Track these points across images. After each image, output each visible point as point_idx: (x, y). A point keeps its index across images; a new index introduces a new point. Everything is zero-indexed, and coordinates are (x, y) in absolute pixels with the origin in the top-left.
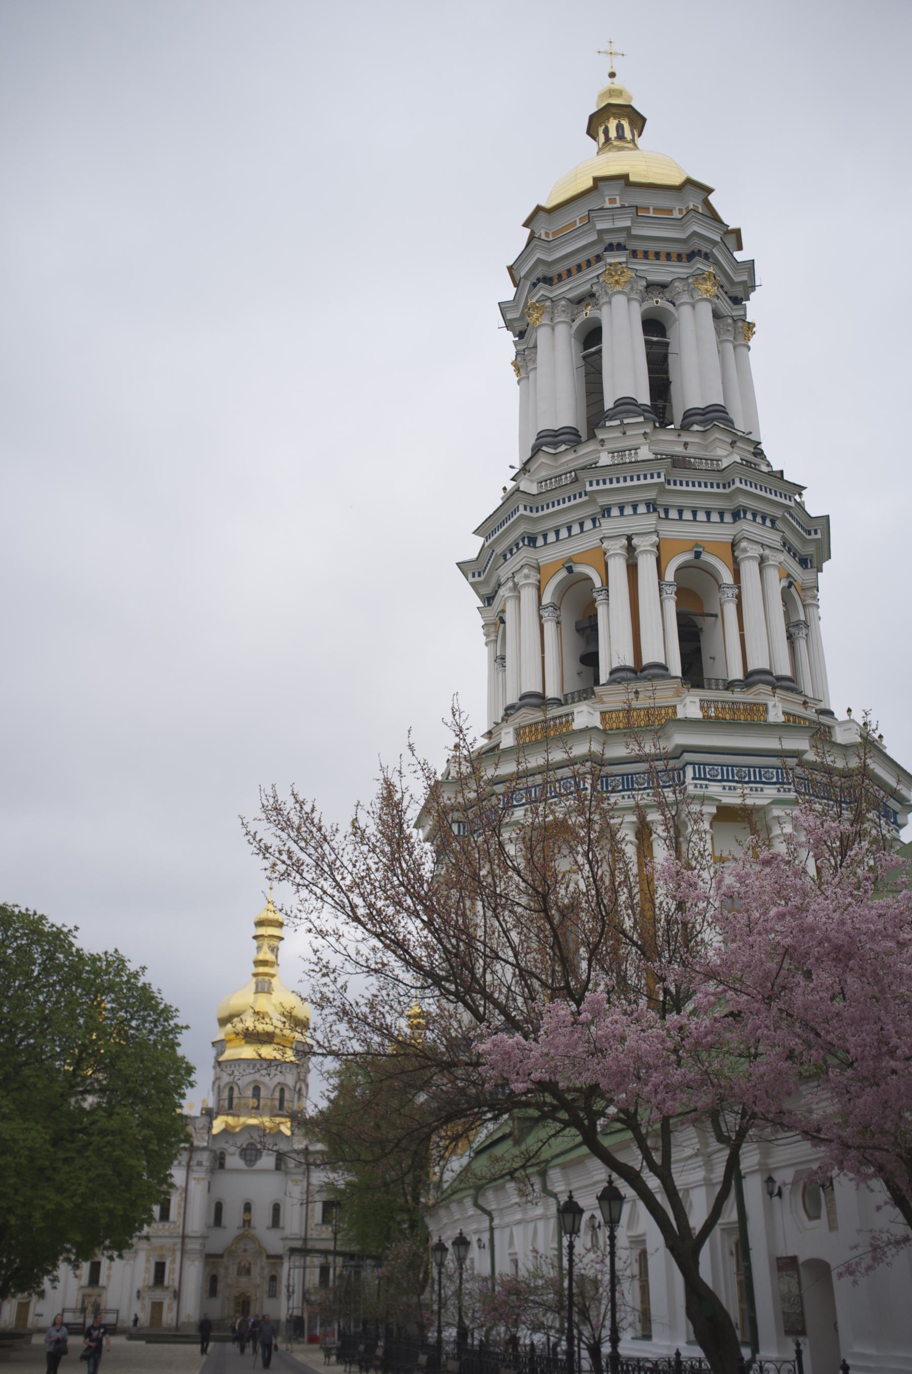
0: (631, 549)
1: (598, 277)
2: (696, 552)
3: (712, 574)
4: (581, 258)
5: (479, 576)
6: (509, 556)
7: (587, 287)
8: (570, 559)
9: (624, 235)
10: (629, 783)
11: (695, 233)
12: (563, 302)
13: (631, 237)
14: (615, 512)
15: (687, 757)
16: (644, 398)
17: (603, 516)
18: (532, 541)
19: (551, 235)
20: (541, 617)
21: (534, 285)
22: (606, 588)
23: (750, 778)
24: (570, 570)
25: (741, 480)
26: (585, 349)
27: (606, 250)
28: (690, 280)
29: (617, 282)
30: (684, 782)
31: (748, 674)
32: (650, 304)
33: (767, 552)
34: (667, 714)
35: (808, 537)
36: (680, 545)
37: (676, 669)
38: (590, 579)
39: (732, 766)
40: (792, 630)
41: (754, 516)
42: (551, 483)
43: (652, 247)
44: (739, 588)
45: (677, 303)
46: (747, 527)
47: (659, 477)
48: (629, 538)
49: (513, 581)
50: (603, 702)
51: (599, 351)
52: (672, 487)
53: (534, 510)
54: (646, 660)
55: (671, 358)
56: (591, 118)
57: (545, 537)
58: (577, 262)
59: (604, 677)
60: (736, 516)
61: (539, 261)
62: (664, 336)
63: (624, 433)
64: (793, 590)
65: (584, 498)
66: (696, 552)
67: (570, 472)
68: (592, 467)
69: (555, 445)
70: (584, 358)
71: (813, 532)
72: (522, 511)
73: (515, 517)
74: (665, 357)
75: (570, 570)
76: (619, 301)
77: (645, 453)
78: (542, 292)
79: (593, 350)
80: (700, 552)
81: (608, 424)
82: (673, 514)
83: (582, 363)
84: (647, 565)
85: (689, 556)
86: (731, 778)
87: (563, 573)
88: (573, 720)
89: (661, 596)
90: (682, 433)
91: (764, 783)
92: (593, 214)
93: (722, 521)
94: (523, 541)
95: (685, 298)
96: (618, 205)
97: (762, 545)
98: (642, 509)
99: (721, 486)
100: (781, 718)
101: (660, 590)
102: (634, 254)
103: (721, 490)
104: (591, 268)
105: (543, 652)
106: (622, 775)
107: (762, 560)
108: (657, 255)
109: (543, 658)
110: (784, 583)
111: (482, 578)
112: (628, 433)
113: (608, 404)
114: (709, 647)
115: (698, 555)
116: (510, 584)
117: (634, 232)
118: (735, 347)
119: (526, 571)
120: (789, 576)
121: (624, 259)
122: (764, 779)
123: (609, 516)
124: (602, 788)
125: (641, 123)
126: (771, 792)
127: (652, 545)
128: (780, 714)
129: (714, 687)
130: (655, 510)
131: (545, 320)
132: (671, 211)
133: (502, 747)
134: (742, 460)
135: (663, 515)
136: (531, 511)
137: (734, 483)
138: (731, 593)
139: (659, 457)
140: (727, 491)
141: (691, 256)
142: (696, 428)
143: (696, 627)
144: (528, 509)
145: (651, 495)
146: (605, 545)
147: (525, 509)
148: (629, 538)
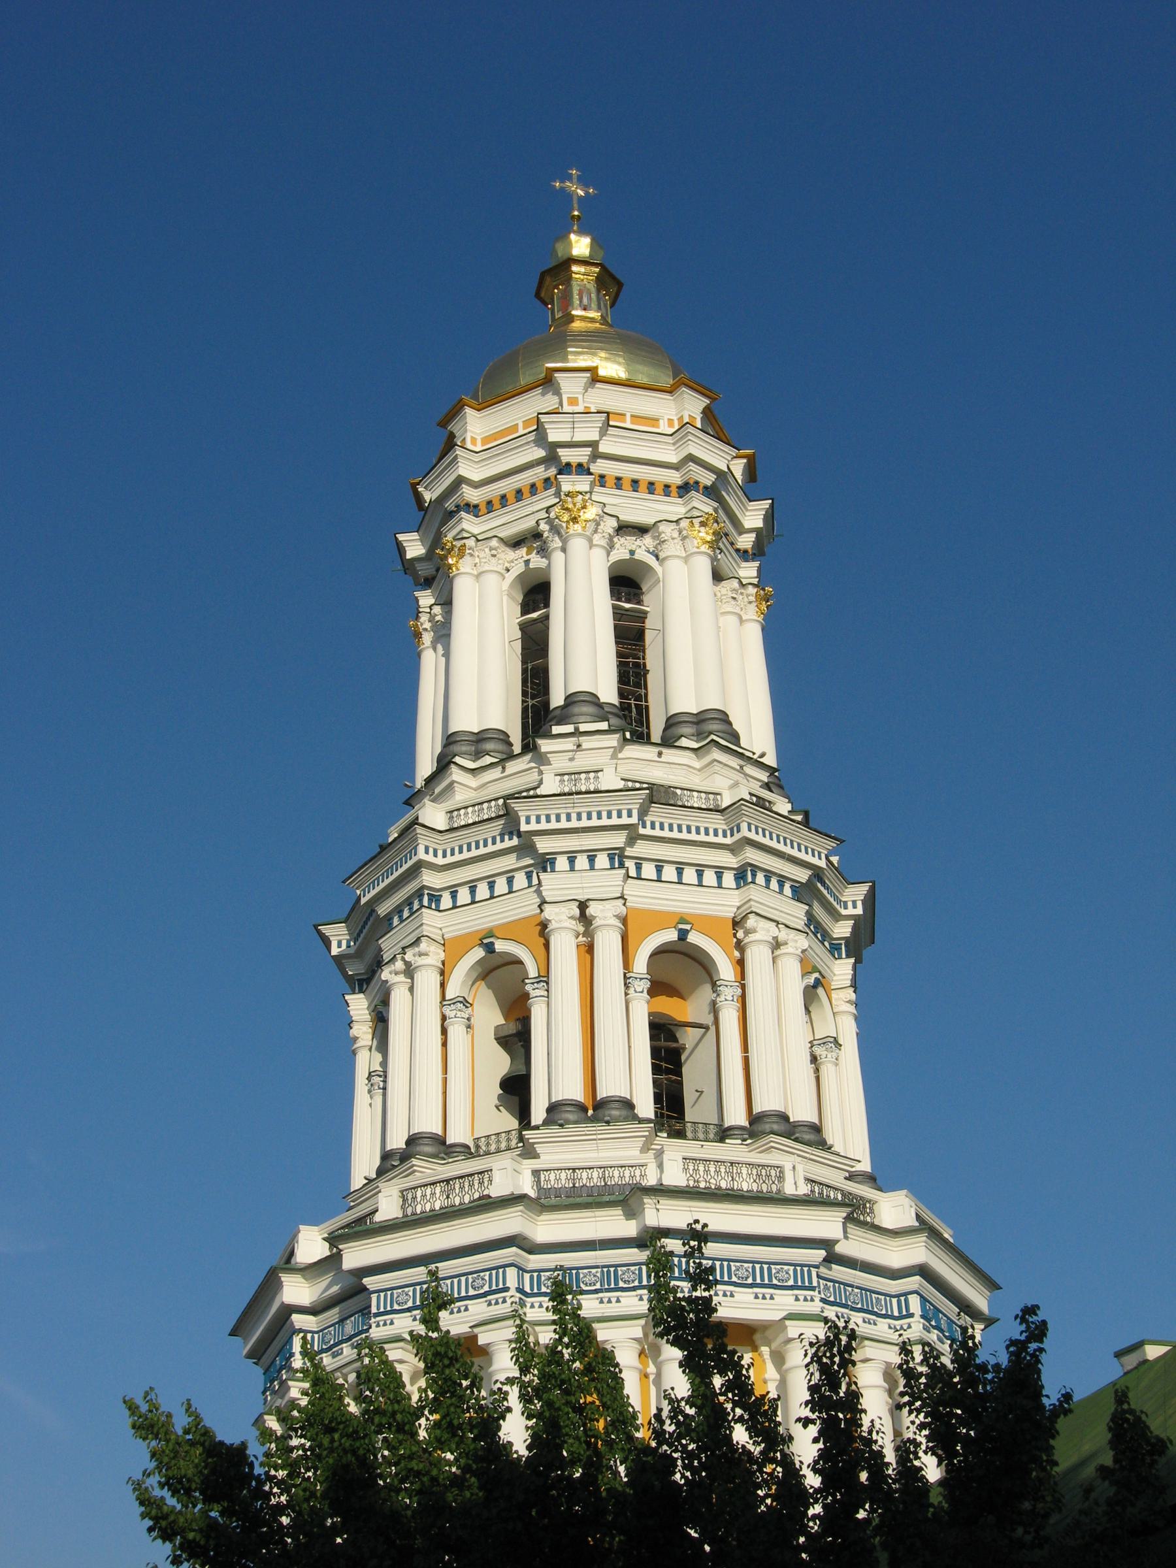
1: (548, 510)
2: (680, 930)
3: (703, 965)
6: (396, 921)
7: (529, 523)
8: (490, 934)
9: (588, 451)
11: (691, 458)
12: (494, 543)
13: (596, 456)
14: (562, 863)
16: (609, 693)
17: (545, 870)
18: (435, 899)
19: (479, 442)
21: (451, 514)
22: (544, 978)
23: (754, 1279)
24: (490, 948)
25: (749, 825)
26: (524, 613)
27: (560, 473)
28: (685, 524)
29: (575, 520)
31: (756, 1119)
33: (783, 934)
35: (844, 912)
36: (658, 920)
37: (646, 1107)
38: (521, 963)
39: (729, 1260)
40: (818, 1051)
41: (768, 880)
42: (466, 814)
44: (743, 987)
45: (662, 555)
46: (760, 896)
47: (630, 815)
48: (583, 906)
49: (403, 959)
50: (535, 1155)
51: (546, 617)
52: (648, 831)
53: (440, 853)
54: (605, 1090)
55: (649, 636)
56: (543, 275)
57: (454, 895)
58: (517, 486)
59: (538, 1113)
61: (460, 481)
62: (639, 602)
63: (579, 746)
64: (820, 991)
66: (680, 930)
67: (496, 799)
68: (530, 794)
69: (478, 755)
70: (523, 627)
71: (850, 904)
72: (421, 855)
73: (410, 863)
74: (640, 635)
76: (577, 545)
77: (610, 780)
78: (465, 525)
80: (687, 932)
81: (556, 730)
82: (649, 870)
83: (519, 634)
84: (608, 944)
85: (672, 935)
86: (726, 1279)
87: (479, 953)
88: (490, 1181)
89: (626, 994)
90: (665, 750)
94: (421, 901)
95: (673, 548)
96: (580, 408)
97: (778, 923)
100: (803, 1189)
101: (627, 986)
104: (535, 498)
105: (445, 1070)
107: (776, 945)
108: (635, 483)
109: (445, 1081)
110: (811, 980)
112: (584, 746)
113: (557, 699)
114: (694, 1075)
115: (683, 935)
117: (603, 448)
120: (815, 969)
121: (586, 488)
122: (775, 1282)
123: (553, 870)
124: (532, 1288)
125: (613, 290)
126: (785, 1302)
127: (617, 916)
128: (801, 1182)
129: (701, 1136)
130: (622, 865)
132: (657, 420)
133: (378, 1218)
134: (751, 794)
135: (633, 873)
136: (435, 855)
137: (738, 831)
138: (729, 994)
139: (630, 784)
140: (728, 841)
141: (685, 489)
142: (684, 742)
143: (676, 1040)
144: (431, 851)
145: (618, 840)
146: (549, 912)
147: (427, 852)
148: (583, 906)
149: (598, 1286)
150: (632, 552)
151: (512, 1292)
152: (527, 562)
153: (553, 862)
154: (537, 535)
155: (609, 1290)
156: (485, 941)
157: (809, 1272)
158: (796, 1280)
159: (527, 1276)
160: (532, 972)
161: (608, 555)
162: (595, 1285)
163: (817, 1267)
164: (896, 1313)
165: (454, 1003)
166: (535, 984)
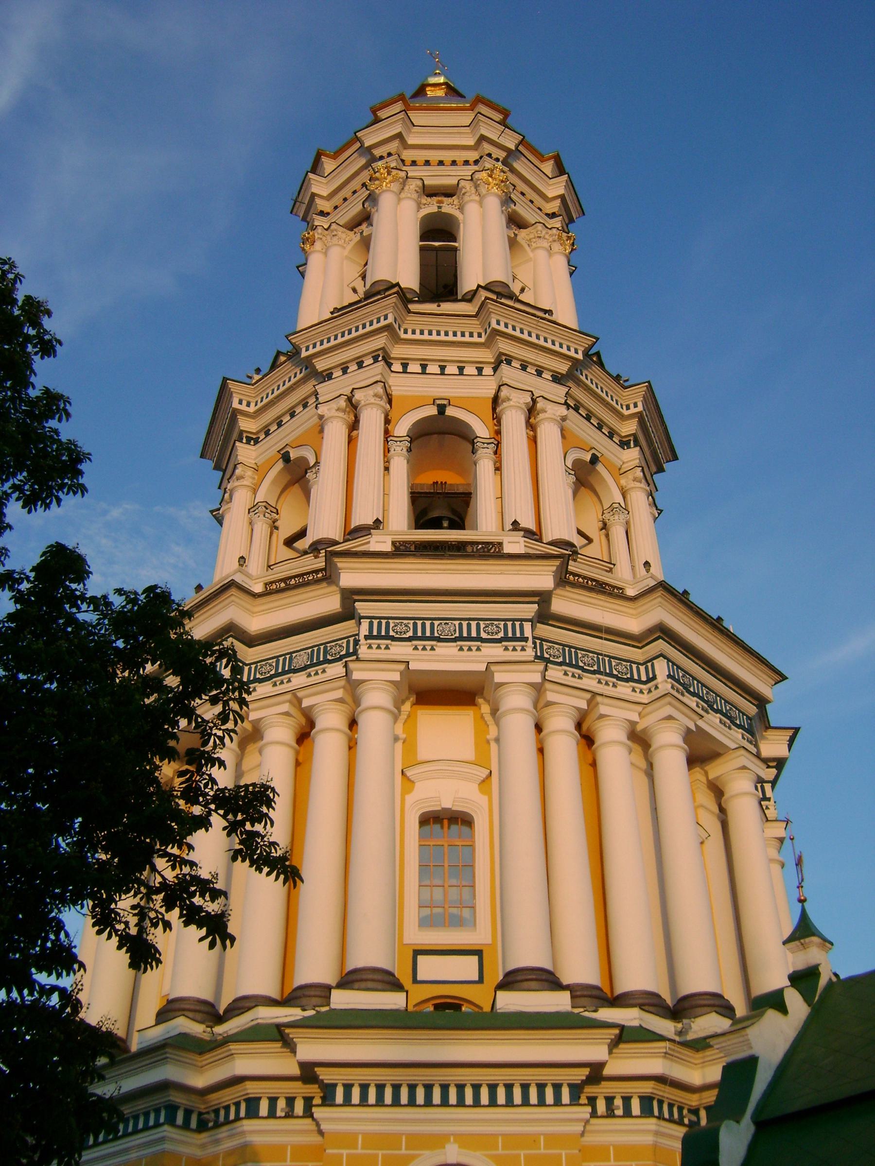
0: (531, 411)
4: (447, 156)
5: (248, 405)
7: (453, 181)
12: (419, 183)
20: (387, 450)
24: (442, 409)
30: (654, 677)
45: (534, 245)
70: (422, 249)
75: (442, 409)
79: (437, 244)
87: (433, 411)
92: (480, 117)
106: (564, 645)
111: (252, 409)
116: (342, 402)
131: (395, 187)
148: (534, 401)
149: (595, 668)
151: (530, 643)
152: (439, 207)
154: (449, 192)
155: (607, 675)
156: (438, 402)
162: (592, 667)
165: (400, 441)
166: (486, 445)
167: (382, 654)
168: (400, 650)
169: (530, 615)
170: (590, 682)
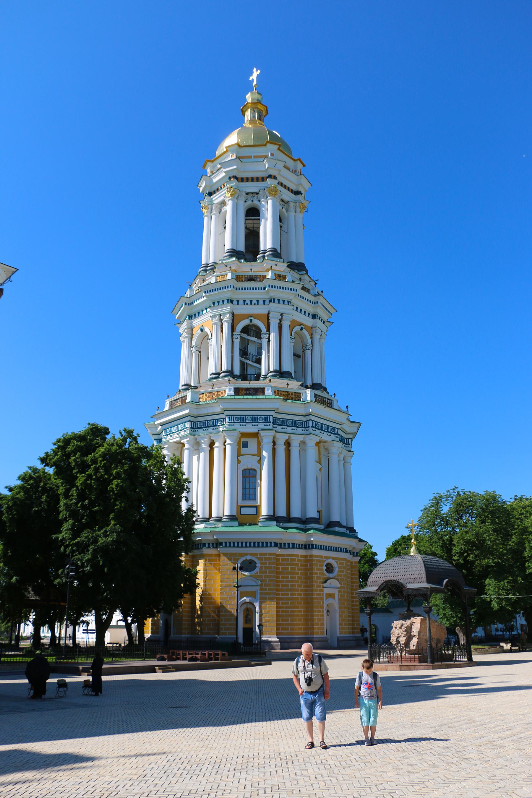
10: (206, 425)
15: (226, 413)
16: (241, 247)
32: (249, 203)
34: (222, 394)
43: (250, 175)
46: (273, 306)
57: (195, 315)
60: (270, 301)
62: (259, 216)
65: (205, 298)
75: (202, 330)
82: (241, 302)
87: (200, 332)
91: (259, 422)
93: (264, 304)
98: (226, 302)
99: (263, 289)
102: (242, 180)
103: (263, 290)
115: (251, 321)
118: (295, 216)
119: (186, 331)
122: (259, 421)
126: (262, 426)
130: (232, 301)
150: (252, 201)
153: (214, 303)
157: (269, 417)
158: (265, 420)
159: (195, 423)
160: (210, 337)
161: (244, 205)
163: (272, 416)
164: (305, 426)
167: (166, 440)
168: (169, 437)
169: (189, 420)
170: (210, 429)
